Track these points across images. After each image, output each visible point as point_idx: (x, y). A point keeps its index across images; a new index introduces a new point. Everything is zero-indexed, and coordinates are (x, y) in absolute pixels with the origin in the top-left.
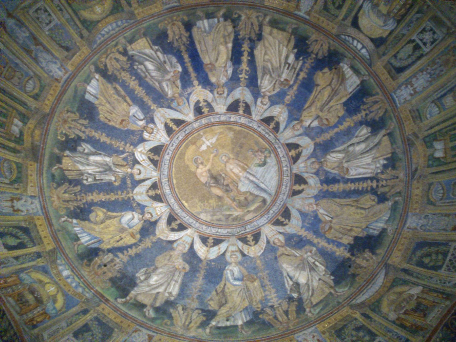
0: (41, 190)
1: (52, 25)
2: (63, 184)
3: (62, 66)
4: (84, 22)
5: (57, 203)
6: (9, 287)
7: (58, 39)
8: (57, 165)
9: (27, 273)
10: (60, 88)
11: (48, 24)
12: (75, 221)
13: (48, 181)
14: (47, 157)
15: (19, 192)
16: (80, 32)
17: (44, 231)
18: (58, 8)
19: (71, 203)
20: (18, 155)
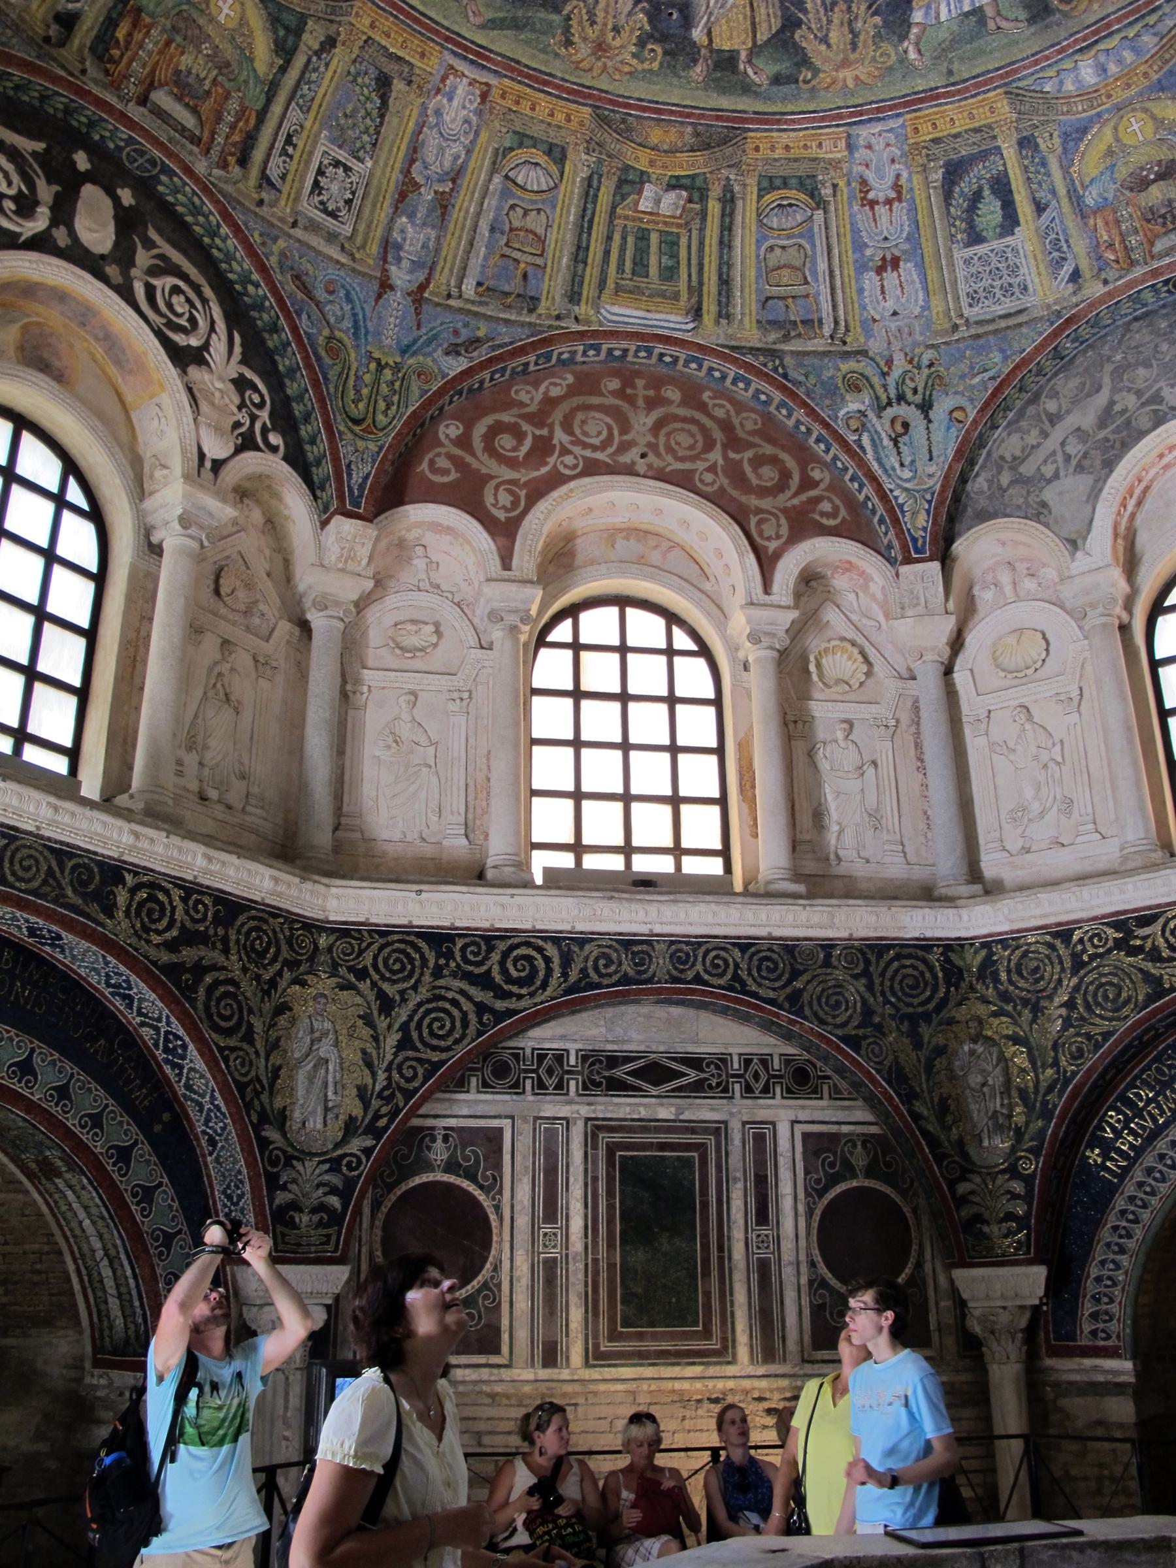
0: (831, 117)
1: (342, 155)
2: (799, 49)
3: (438, 91)
4: (285, 51)
5: (862, 71)
6: (1123, 241)
7: (368, 121)
8: (742, 67)
9: (1085, 188)
10: (506, 81)
11: (347, 169)
12: (918, 16)
13: (796, 97)
14: (725, 102)
15: (842, 184)
16: (318, 53)
17: (954, 118)
18: (290, 150)
19: (860, 24)
20: (737, 188)
